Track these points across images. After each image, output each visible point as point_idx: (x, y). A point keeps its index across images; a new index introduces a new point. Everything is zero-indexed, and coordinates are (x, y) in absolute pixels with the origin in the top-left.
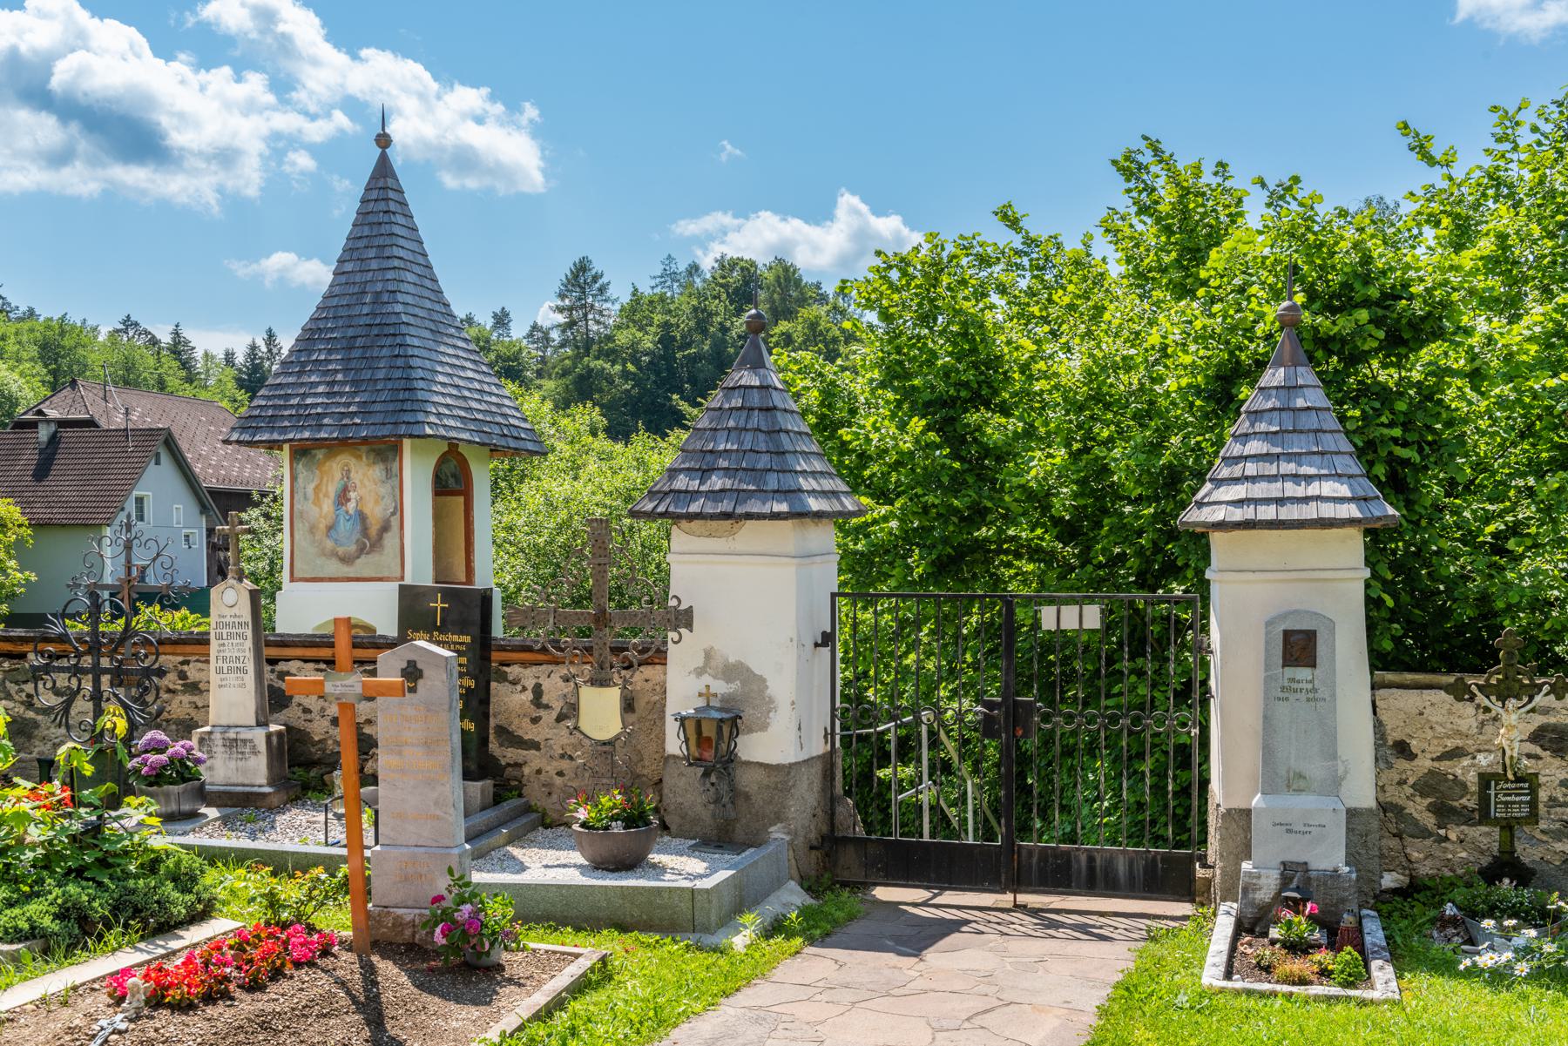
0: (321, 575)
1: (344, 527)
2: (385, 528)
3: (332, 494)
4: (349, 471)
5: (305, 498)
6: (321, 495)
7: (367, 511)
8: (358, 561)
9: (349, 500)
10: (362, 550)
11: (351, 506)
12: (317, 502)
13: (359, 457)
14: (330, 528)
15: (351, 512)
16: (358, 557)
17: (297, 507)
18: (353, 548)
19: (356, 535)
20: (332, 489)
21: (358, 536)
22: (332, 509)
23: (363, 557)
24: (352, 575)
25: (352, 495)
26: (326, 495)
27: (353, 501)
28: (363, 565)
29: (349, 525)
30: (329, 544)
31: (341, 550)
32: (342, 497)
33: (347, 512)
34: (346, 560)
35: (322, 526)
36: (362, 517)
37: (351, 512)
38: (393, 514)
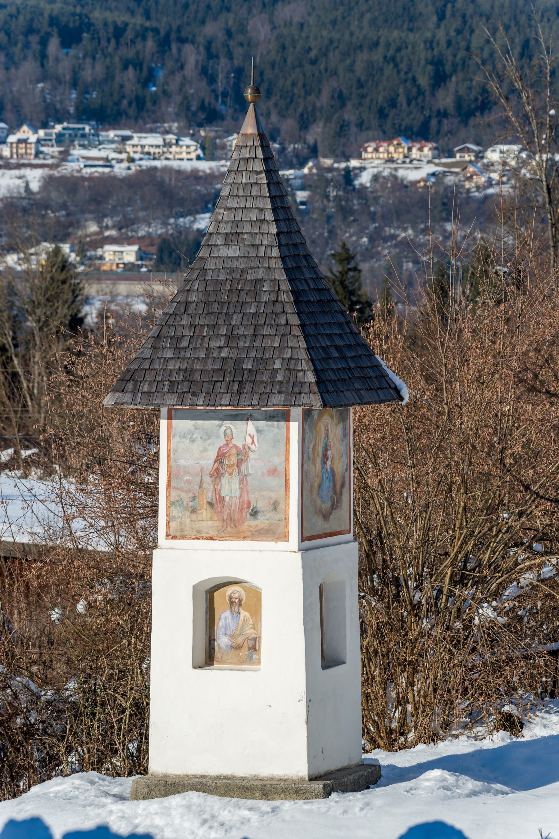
0: (314, 533)
1: (326, 484)
3: (320, 454)
4: (328, 430)
7: (335, 469)
8: (332, 517)
9: (327, 459)
11: (329, 463)
14: (320, 486)
16: (331, 513)
17: (305, 466)
18: (328, 505)
19: (331, 493)
25: (329, 453)
26: (318, 455)
27: (330, 459)
29: (327, 481)
32: (325, 458)
35: (316, 485)
37: (329, 470)
38: (346, 470)
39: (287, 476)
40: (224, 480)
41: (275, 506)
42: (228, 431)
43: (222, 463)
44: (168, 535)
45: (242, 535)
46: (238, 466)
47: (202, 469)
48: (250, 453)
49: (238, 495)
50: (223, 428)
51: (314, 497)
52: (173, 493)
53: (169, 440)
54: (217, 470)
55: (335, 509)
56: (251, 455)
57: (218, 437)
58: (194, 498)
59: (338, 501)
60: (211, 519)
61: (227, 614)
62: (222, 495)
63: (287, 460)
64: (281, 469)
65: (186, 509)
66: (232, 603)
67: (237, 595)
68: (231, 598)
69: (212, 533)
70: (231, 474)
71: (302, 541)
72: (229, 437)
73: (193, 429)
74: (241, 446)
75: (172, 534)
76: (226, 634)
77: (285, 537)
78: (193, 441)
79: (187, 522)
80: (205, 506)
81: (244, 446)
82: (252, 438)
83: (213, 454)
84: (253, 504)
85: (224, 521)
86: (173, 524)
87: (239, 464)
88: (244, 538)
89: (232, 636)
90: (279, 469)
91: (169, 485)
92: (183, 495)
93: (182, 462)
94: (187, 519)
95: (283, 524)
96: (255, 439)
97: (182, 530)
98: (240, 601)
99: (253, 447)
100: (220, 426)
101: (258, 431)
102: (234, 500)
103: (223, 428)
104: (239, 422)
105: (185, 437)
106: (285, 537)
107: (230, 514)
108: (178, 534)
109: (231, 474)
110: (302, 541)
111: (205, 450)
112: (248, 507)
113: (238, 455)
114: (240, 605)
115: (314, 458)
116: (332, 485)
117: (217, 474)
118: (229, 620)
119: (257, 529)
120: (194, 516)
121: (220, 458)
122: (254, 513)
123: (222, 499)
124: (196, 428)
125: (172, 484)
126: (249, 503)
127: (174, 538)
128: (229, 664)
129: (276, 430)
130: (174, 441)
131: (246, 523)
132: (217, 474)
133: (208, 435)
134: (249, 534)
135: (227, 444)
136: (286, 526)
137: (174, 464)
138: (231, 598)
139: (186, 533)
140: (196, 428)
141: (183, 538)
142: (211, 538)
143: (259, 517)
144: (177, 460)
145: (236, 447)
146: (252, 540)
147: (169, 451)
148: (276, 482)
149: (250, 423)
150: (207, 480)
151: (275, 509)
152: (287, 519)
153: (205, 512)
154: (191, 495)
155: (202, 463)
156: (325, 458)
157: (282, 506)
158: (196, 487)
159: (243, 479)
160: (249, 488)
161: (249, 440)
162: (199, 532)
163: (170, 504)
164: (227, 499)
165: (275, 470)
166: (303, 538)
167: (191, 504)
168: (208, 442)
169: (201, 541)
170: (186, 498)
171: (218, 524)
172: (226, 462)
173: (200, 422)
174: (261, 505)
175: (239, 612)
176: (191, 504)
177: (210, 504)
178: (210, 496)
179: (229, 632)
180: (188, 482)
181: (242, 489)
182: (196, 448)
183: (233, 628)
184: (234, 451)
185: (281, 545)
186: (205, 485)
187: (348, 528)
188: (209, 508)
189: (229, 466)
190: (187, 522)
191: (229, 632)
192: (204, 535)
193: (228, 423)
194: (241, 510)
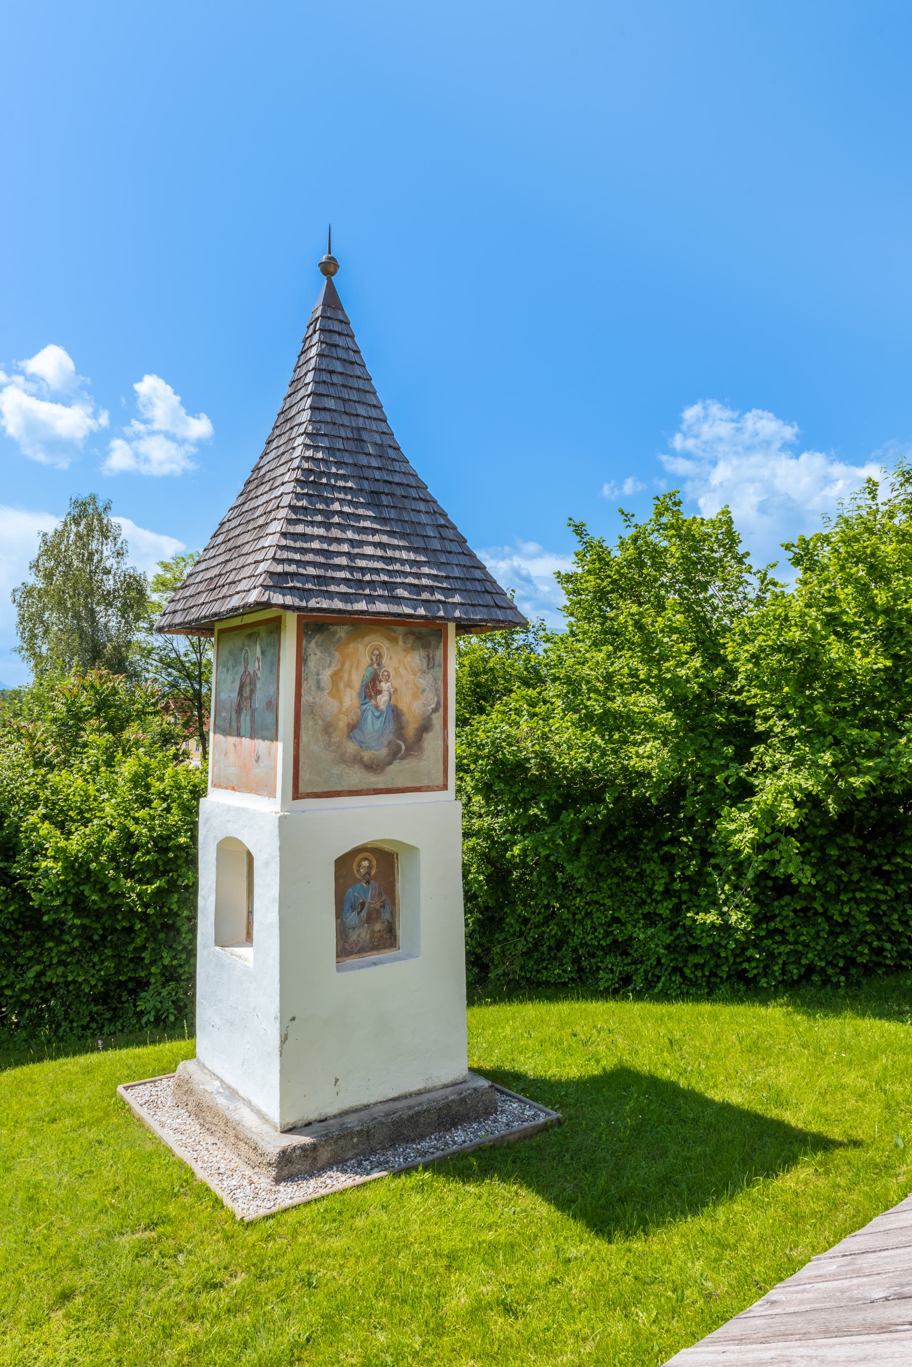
0: (338, 788)
2: (425, 727)
4: (380, 656)
5: (319, 687)
6: (341, 685)
7: (403, 706)
8: (390, 769)
9: (380, 692)
10: (395, 755)
11: (382, 700)
12: (336, 693)
13: (394, 640)
14: (353, 727)
15: (382, 707)
17: (305, 698)
18: (383, 752)
19: (389, 736)
20: (357, 678)
21: (391, 737)
22: (357, 702)
23: (396, 762)
24: (381, 786)
25: (384, 686)
26: (349, 685)
28: (396, 773)
29: (378, 724)
30: (351, 748)
31: (367, 755)
32: (371, 689)
33: (377, 707)
34: (373, 767)
35: (342, 724)
36: (396, 713)
37: (382, 707)
38: (435, 710)
51: (335, 739)
55: (402, 758)
56: (259, 685)
64: (274, 702)
71: (297, 796)
116: (391, 726)
142: (233, 789)
152: (275, 767)
156: (371, 689)
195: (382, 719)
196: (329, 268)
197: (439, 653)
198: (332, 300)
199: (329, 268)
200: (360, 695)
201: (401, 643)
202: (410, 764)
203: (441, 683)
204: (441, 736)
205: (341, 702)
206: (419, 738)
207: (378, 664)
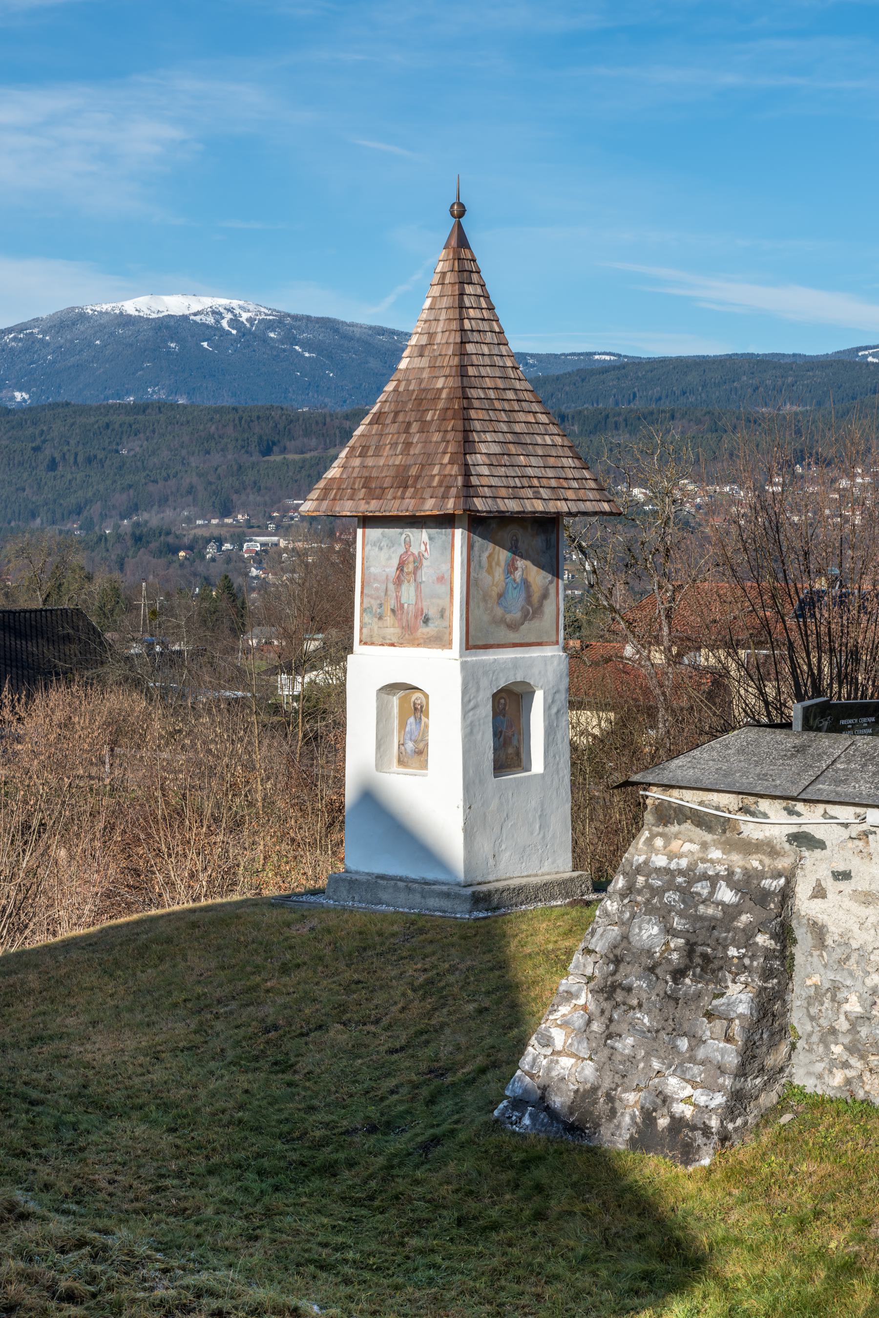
0: (491, 642)
2: (545, 596)
3: (503, 563)
4: (517, 540)
6: (494, 564)
7: (530, 579)
9: (516, 569)
10: (526, 617)
11: (518, 574)
12: (490, 571)
14: (501, 596)
15: (518, 580)
16: (522, 624)
18: (518, 615)
21: (523, 603)
22: (502, 578)
23: (526, 623)
26: (498, 564)
27: (520, 569)
28: (528, 631)
30: (499, 611)
31: (508, 617)
33: (515, 580)
34: (513, 627)
37: (518, 580)
39: (451, 583)
40: (404, 587)
41: (442, 614)
42: (408, 539)
43: (402, 570)
44: (361, 641)
45: (416, 642)
46: (415, 573)
47: (387, 576)
48: (424, 561)
49: (414, 603)
50: (404, 536)
51: (490, 606)
52: (365, 600)
53: (363, 548)
54: (398, 577)
55: (531, 620)
56: (425, 563)
57: (400, 544)
58: (381, 605)
59: (534, 612)
60: (393, 626)
61: (412, 720)
62: (402, 602)
63: (452, 567)
64: (447, 576)
65: (375, 615)
66: (416, 709)
67: (419, 702)
68: (415, 704)
69: (394, 640)
70: (409, 582)
71: (467, 649)
72: (408, 544)
73: (381, 537)
74: (416, 554)
75: (364, 640)
76: (411, 740)
77: (449, 645)
78: (381, 549)
79: (376, 628)
80: (389, 613)
81: (419, 553)
82: (426, 545)
83: (395, 562)
84: (425, 611)
85: (403, 628)
86: (365, 631)
87: (415, 572)
88: (418, 645)
89: (415, 741)
90: (446, 577)
91: (362, 592)
92: (373, 602)
93: (372, 569)
94: (375, 624)
95: (447, 631)
96: (428, 547)
97: (371, 636)
98: (422, 707)
99: (426, 554)
100: (401, 534)
101: (430, 539)
102: (411, 608)
103: (404, 536)
104: (415, 530)
105: (375, 545)
106: (449, 645)
107: (407, 621)
108: (368, 640)
109: (409, 582)
110: (467, 649)
111: (390, 558)
112: (422, 614)
113: (414, 562)
114: (422, 711)
115: (490, 566)
117: (398, 582)
118: (414, 726)
119: (429, 636)
120: (380, 624)
121: (401, 567)
122: (426, 621)
123: (402, 606)
124: (384, 537)
125: (365, 591)
126: (422, 609)
127: (365, 644)
128: (413, 768)
129: (444, 537)
130: (368, 548)
131: (420, 631)
132: (398, 582)
133: (392, 544)
134: (422, 641)
135: (407, 552)
136: (450, 633)
137: (366, 572)
138: (415, 704)
139: (374, 639)
140: (384, 537)
141: (372, 644)
142: (393, 645)
143: (430, 624)
144: (369, 567)
145: (413, 554)
146: (424, 647)
147: (363, 558)
148: (443, 589)
149: (424, 530)
150: (391, 587)
151: (442, 616)
152: (450, 627)
153: (389, 619)
154: (379, 602)
155: (387, 570)
157: (447, 614)
158: (383, 594)
159: (418, 586)
160: (423, 595)
161: (423, 548)
162: (384, 638)
163: (363, 611)
164: (406, 605)
165: (443, 577)
166: (469, 645)
167: (378, 610)
168: (392, 549)
169: (386, 648)
170: (375, 604)
171: (398, 630)
172: (405, 570)
173: (386, 530)
174: (432, 612)
175: (420, 718)
176: (378, 610)
177: (393, 611)
178: (392, 603)
179: (413, 738)
180: (377, 589)
181: (417, 596)
182: (383, 555)
183: (416, 733)
184: (411, 559)
185: (446, 652)
186: (389, 593)
187: (554, 639)
188: (392, 616)
189: (408, 574)
190: (376, 628)
191: (413, 738)
192: (388, 641)
193: (407, 531)
194: (416, 617)
195: (518, 589)
196: (459, 211)
197: (554, 536)
198: (461, 241)
199: (459, 211)
200: (504, 571)
201: (529, 530)
202: (535, 624)
203: (554, 560)
204: (554, 604)
205: (493, 577)
206: (541, 605)
207: (516, 547)
